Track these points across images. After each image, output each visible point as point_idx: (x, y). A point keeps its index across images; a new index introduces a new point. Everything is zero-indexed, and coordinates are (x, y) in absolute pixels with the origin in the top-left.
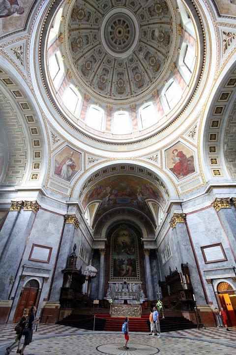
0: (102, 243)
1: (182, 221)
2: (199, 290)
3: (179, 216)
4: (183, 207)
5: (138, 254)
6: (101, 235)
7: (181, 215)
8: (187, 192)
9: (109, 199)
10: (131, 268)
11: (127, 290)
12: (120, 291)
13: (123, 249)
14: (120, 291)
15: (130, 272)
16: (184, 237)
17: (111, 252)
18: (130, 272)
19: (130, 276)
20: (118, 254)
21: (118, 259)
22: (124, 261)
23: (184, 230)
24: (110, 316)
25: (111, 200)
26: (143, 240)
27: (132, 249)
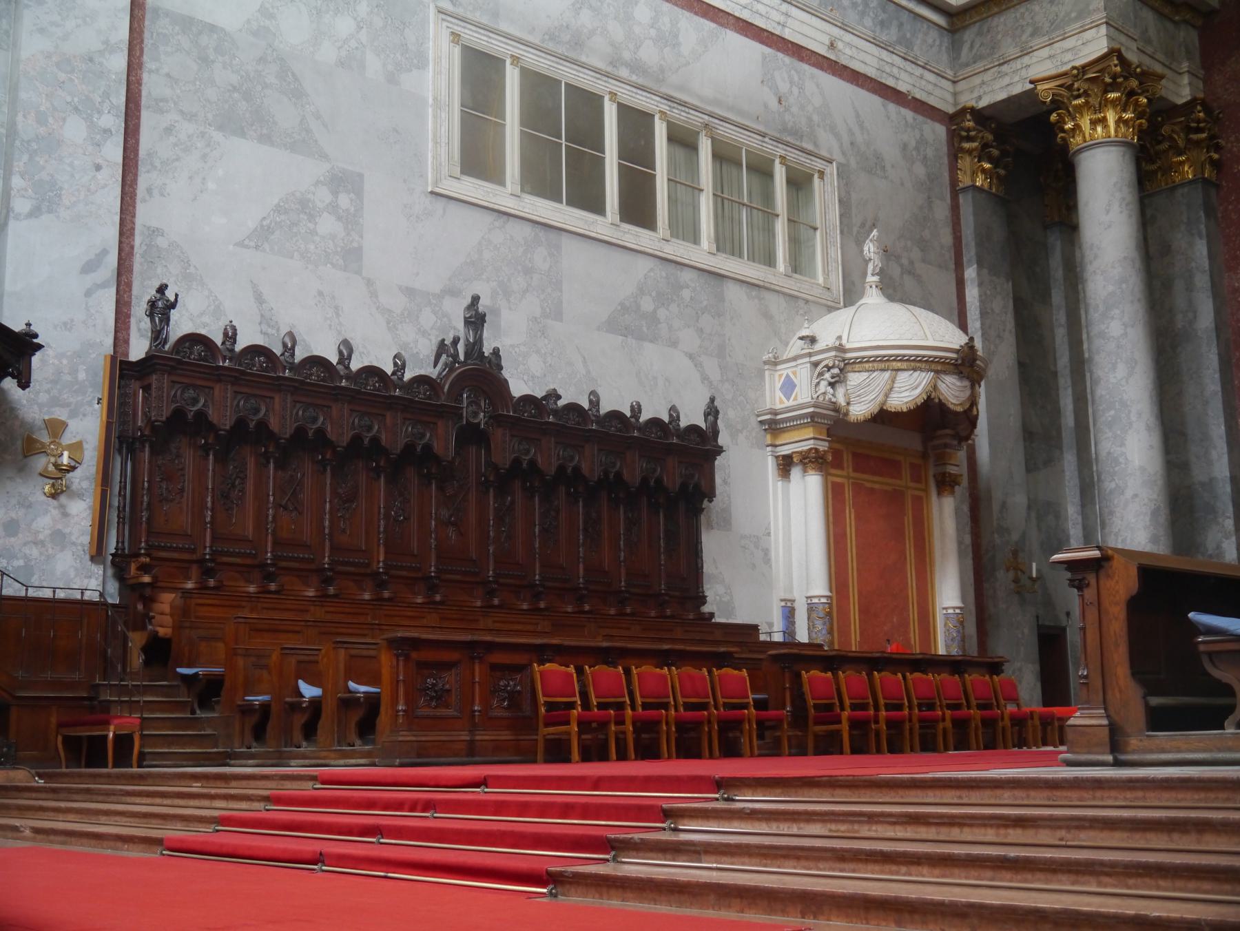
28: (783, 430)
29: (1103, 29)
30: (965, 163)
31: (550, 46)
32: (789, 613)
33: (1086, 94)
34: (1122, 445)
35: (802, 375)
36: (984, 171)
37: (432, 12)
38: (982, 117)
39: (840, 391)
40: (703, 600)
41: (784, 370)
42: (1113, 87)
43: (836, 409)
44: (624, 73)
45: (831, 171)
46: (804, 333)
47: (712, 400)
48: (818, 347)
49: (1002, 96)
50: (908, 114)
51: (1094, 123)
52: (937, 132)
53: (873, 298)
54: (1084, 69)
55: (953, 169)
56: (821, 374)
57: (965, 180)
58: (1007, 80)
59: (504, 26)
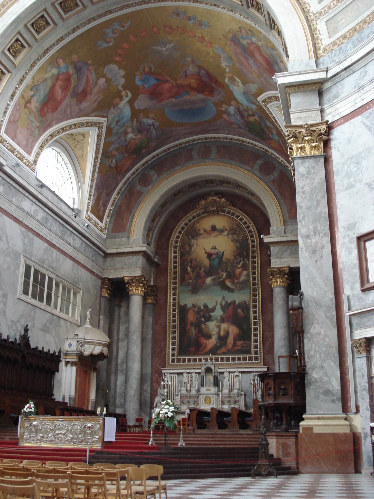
0: (134, 258)
1: (314, 152)
2: (326, 374)
3: (304, 131)
4: (326, 98)
5: (259, 287)
6: (129, 237)
7: (309, 128)
8: (344, 37)
9: (135, 113)
10: (233, 330)
11: (213, 390)
12: (193, 392)
13: (208, 274)
14: (193, 392)
15: (231, 340)
16: (309, 208)
17: (171, 286)
18: (231, 340)
19: (229, 352)
20: (195, 290)
21: (194, 306)
22: (213, 310)
23: (316, 181)
24: (16, 444)
25: (146, 112)
26: (267, 239)
27: (240, 274)
28: (68, 355)
29: (141, 269)
30: (104, 290)
31: (39, 263)
32: (64, 398)
33: (135, 283)
34: (133, 365)
35: (74, 343)
36: (108, 293)
37: (22, 255)
38: (109, 280)
39: (83, 348)
40: (53, 395)
41: (69, 341)
42: (141, 283)
43: (81, 352)
44: (50, 269)
45: (81, 292)
46: (76, 333)
47: (60, 349)
48: (79, 337)
49: (115, 277)
50: (95, 277)
51: (136, 290)
52: (99, 282)
53: (88, 325)
54: (135, 277)
55: (101, 291)
56: (79, 344)
57: (103, 294)
58: (116, 273)
59: (33, 259)
